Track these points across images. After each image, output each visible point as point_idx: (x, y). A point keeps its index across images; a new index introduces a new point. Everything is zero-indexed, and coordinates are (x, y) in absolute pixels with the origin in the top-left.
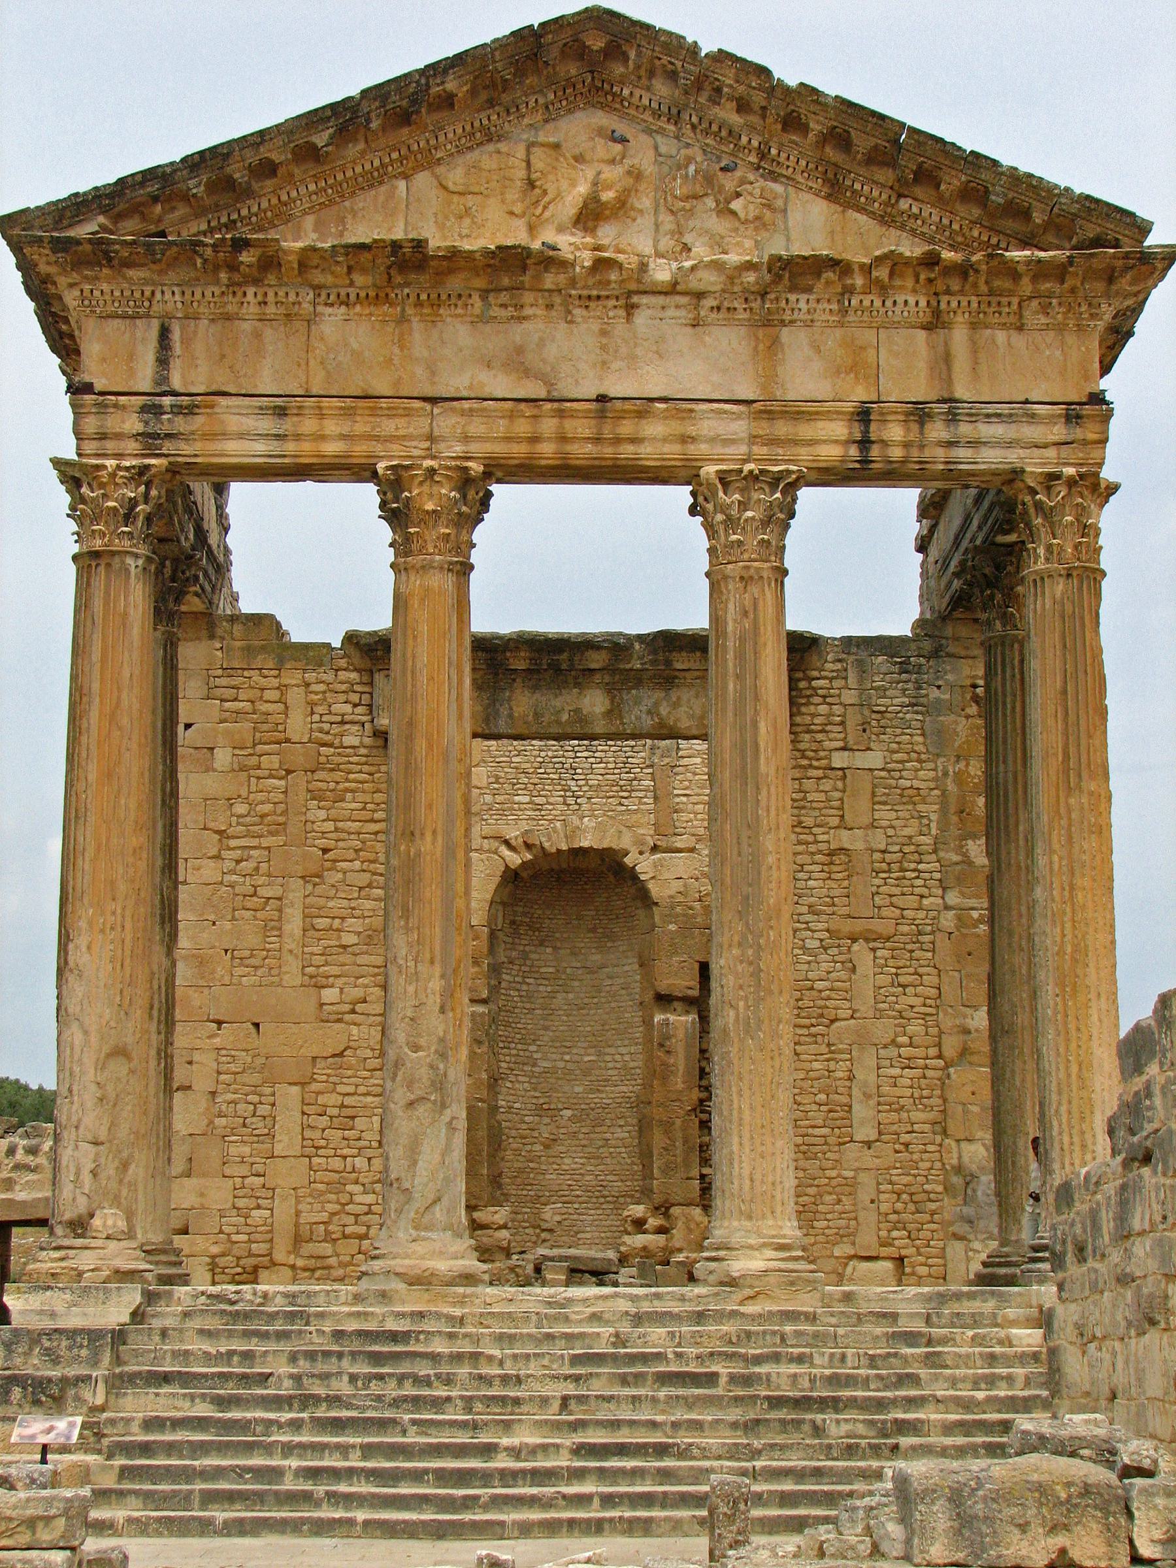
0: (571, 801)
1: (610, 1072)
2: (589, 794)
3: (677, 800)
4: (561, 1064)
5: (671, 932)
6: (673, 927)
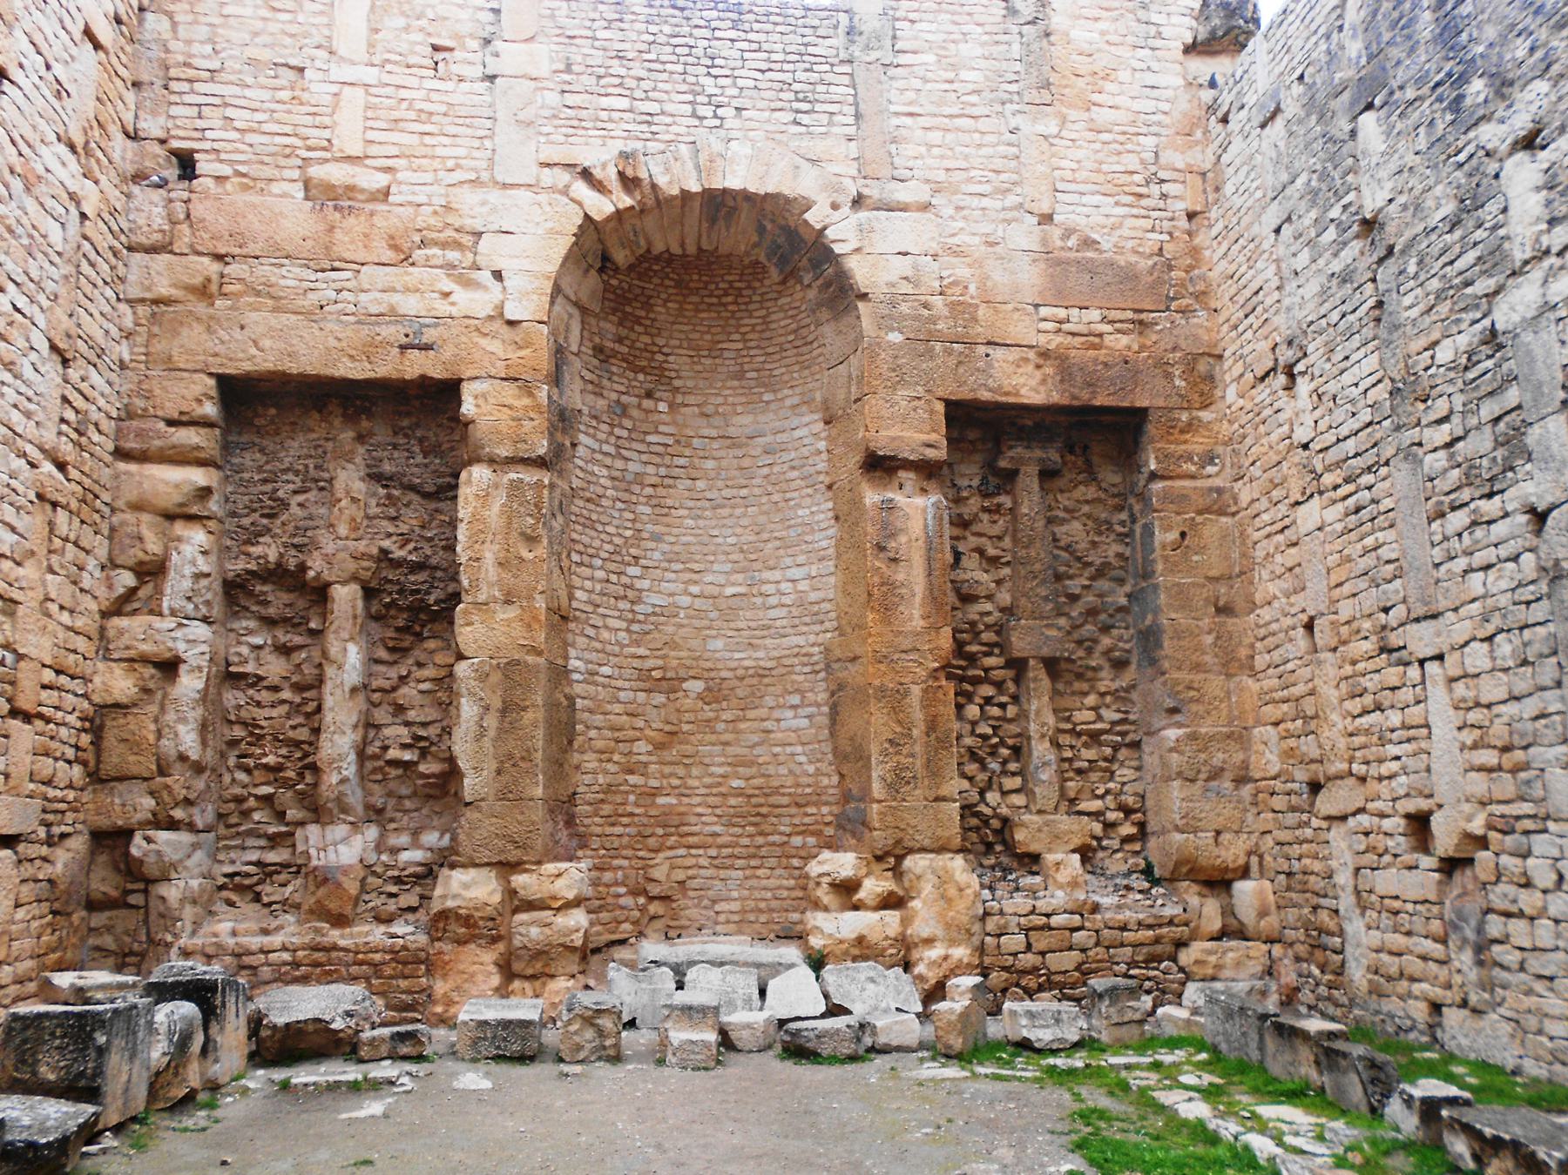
0: (702, 111)
1: (773, 613)
2: (735, 103)
3: (896, 121)
4: (685, 601)
5: (892, 345)
6: (895, 337)
